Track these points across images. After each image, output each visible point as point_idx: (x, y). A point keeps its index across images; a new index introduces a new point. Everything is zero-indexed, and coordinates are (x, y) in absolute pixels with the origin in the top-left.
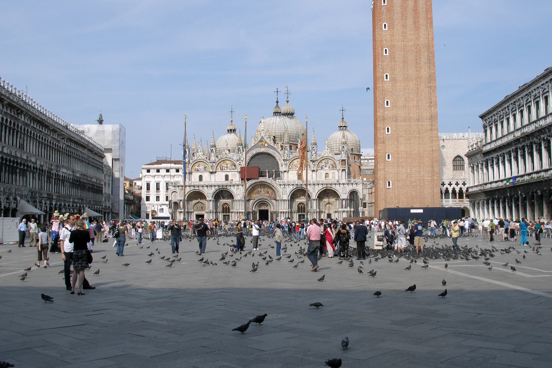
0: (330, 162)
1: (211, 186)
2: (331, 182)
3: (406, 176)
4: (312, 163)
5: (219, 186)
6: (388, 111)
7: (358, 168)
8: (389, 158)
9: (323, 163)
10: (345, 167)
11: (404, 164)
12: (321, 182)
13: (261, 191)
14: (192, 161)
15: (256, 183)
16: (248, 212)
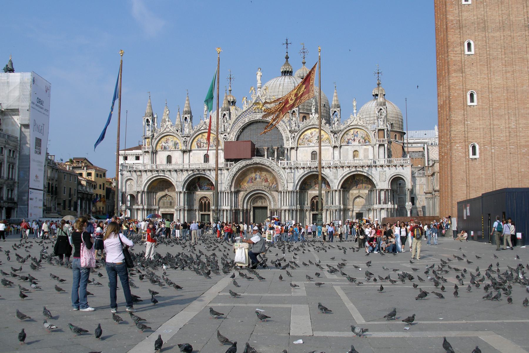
0: (361, 133)
1: (182, 170)
2: (362, 164)
3: (508, 134)
4: (332, 135)
5: (193, 170)
6: (467, 11)
7: (402, 149)
8: (472, 100)
9: (350, 136)
10: (383, 141)
11: (502, 112)
12: (346, 164)
13: (256, 179)
14: (157, 135)
15: (247, 165)
16: (236, 210)
